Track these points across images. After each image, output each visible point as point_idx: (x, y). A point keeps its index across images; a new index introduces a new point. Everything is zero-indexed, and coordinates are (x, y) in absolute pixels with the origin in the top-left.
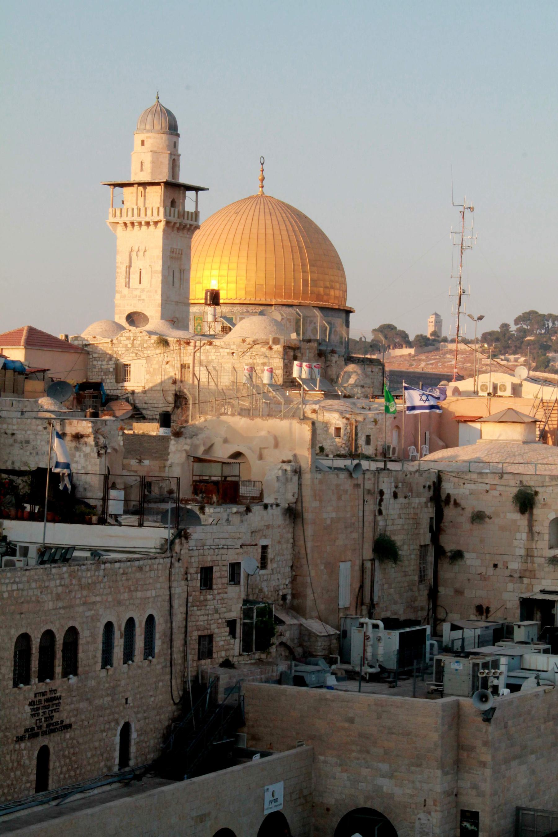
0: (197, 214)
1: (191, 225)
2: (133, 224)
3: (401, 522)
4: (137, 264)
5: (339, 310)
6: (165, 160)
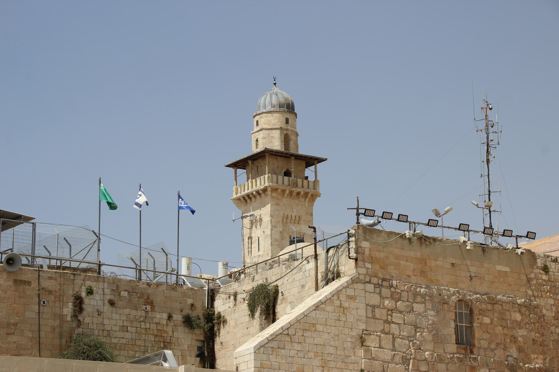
0: (316, 182)
2: (248, 196)
3: (128, 335)
6: (277, 134)
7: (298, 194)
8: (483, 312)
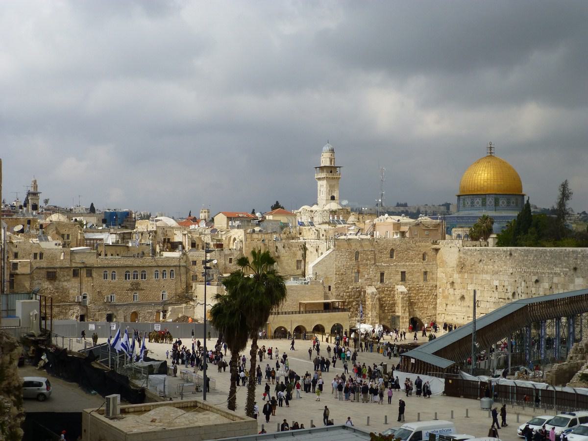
0: (340, 174)
4: (322, 189)
5: (520, 195)
6: (328, 160)
7: (334, 178)
8: (361, 253)
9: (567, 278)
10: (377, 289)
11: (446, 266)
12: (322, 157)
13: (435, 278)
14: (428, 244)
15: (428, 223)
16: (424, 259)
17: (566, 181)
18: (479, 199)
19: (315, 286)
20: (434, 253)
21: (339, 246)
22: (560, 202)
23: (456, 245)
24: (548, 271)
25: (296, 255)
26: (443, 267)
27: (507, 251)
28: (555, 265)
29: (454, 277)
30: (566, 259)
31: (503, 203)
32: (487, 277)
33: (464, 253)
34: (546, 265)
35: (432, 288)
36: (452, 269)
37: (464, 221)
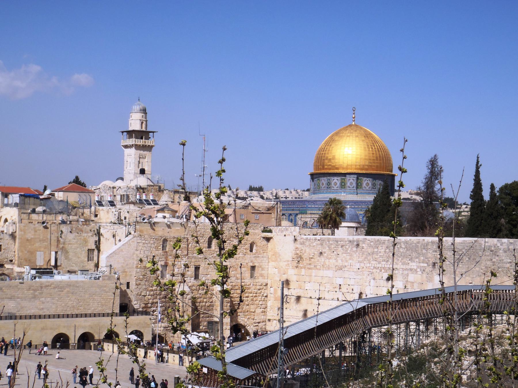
1: (149, 146)
3: (75, 241)
5: (389, 175)
8: (170, 241)
9: (425, 275)
10: (189, 287)
11: (279, 259)
12: (131, 119)
13: (266, 275)
14: (257, 231)
15: (258, 205)
16: (251, 251)
17: (435, 156)
18: (338, 180)
19: (108, 282)
20: (265, 242)
21: (141, 231)
22: (427, 182)
23: (291, 232)
24: (402, 267)
25: (86, 242)
26: (276, 261)
27: (353, 241)
28: (411, 260)
29: (289, 273)
30: (424, 251)
31: (367, 184)
32: (329, 273)
33: (301, 244)
34: (400, 259)
35: (261, 287)
36: (286, 263)
37: (316, 206)
